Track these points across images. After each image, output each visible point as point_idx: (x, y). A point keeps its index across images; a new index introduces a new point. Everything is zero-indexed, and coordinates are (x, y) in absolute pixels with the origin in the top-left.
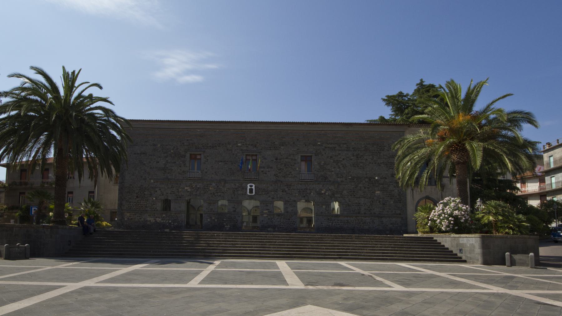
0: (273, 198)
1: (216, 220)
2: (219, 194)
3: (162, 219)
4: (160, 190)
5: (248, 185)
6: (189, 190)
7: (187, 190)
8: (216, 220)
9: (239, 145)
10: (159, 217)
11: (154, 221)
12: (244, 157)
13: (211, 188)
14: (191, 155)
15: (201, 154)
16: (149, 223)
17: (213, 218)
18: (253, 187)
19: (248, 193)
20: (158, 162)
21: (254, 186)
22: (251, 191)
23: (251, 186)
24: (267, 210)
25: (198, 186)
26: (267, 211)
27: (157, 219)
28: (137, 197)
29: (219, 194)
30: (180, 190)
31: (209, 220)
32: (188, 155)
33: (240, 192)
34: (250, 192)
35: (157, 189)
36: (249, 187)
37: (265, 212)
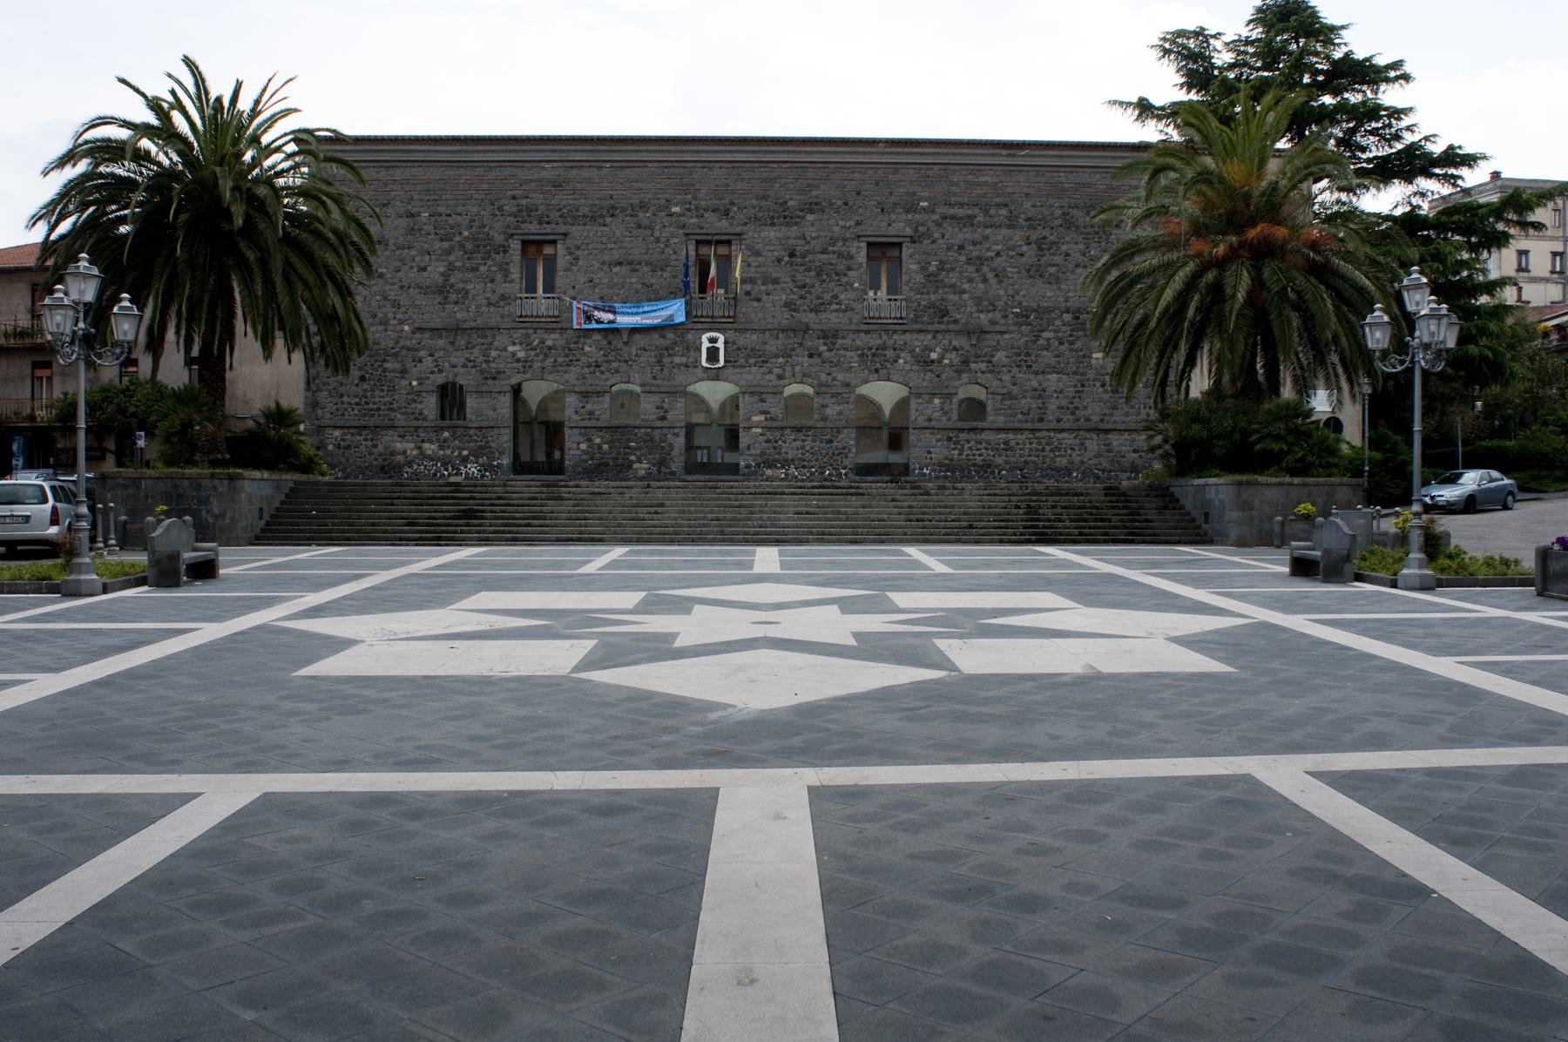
0: (780, 377)
1: (605, 447)
2: (615, 365)
3: (441, 448)
4: (432, 355)
5: (705, 338)
6: (521, 354)
7: (513, 354)
8: (605, 447)
9: (676, 209)
10: (431, 442)
11: (415, 452)
12: (692, 247)
13: (587, 349)
14: (524, 243)
15: (554, 242)
16: (400, 458)
17: (597, 441)
18: (720, 345)
19: (704, 363)
20: (424, 269)
21: (721, 339)
22: (713, 354)
23: (713, 340)
24: (762, 412)
25: (549, 343)
26: (762, 418)
27: (426, 445)
28: (363, 379)
29: (615, 365)
30: (494, 353)
31: (583, 446)
32: (516, 245)
33: (677, 360)
34: (709, 360)
35: (422, 353)
36: (706, 345)
37: (755, 419)
